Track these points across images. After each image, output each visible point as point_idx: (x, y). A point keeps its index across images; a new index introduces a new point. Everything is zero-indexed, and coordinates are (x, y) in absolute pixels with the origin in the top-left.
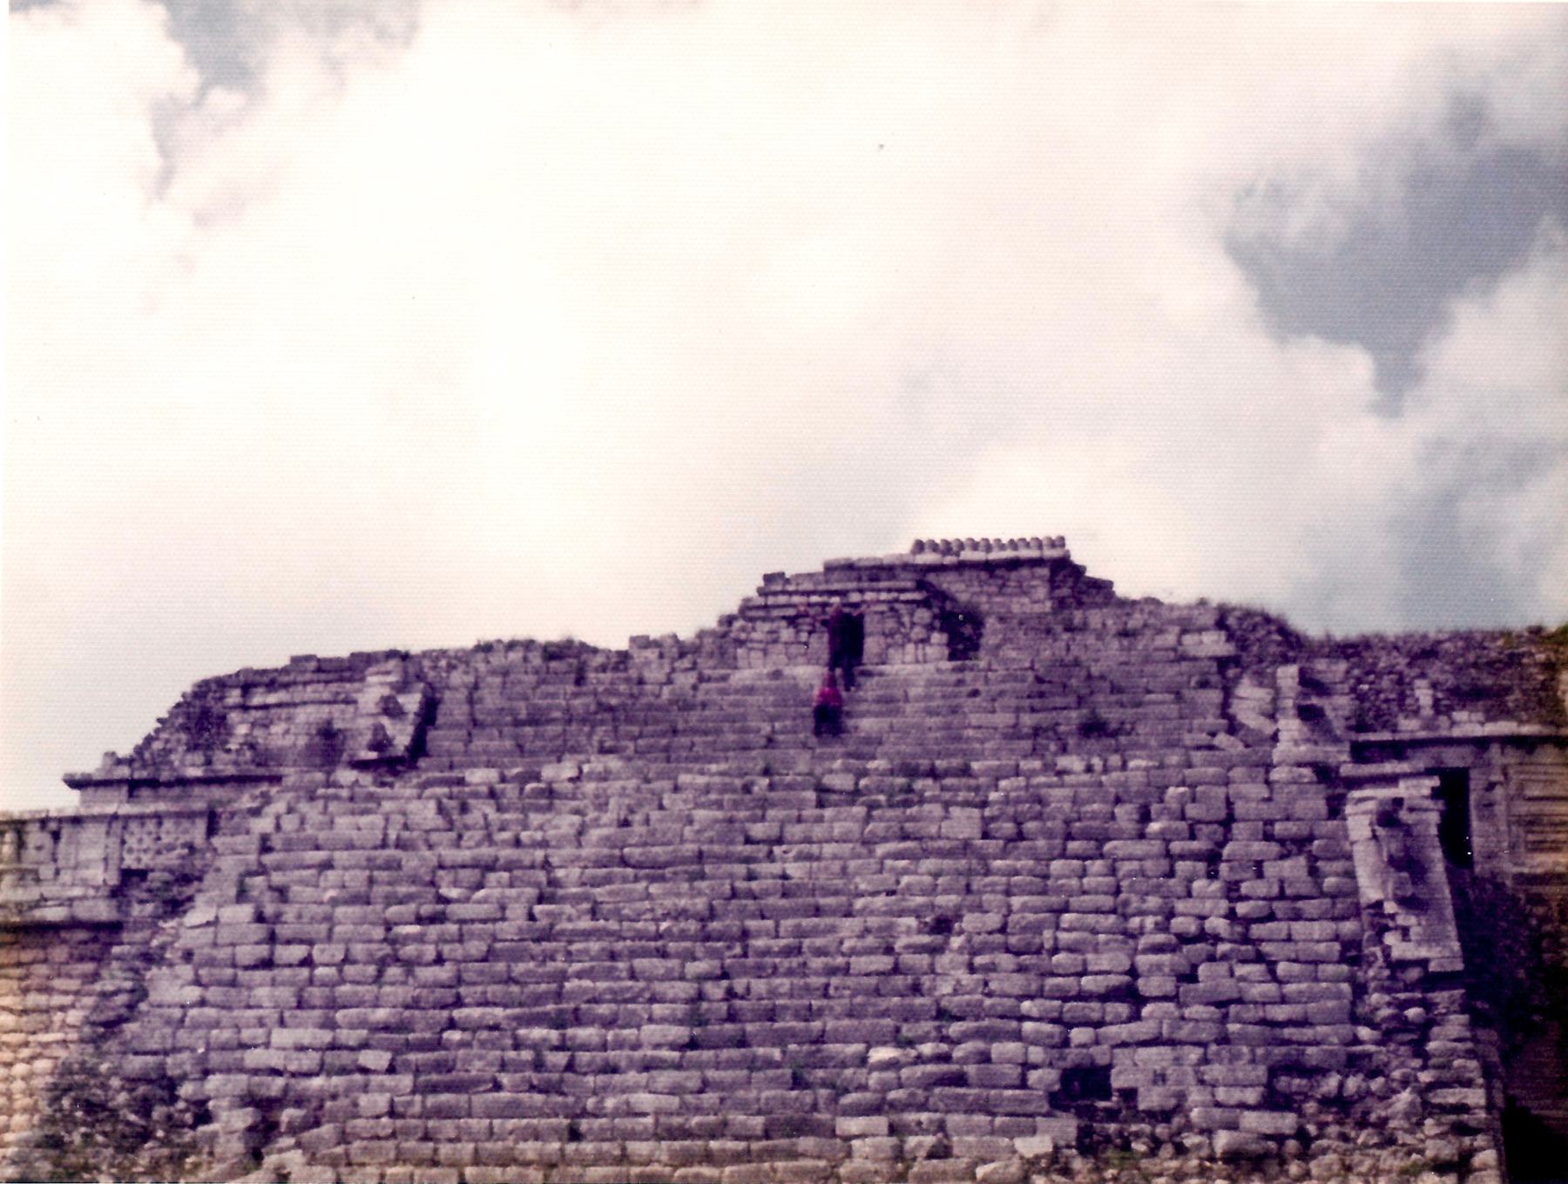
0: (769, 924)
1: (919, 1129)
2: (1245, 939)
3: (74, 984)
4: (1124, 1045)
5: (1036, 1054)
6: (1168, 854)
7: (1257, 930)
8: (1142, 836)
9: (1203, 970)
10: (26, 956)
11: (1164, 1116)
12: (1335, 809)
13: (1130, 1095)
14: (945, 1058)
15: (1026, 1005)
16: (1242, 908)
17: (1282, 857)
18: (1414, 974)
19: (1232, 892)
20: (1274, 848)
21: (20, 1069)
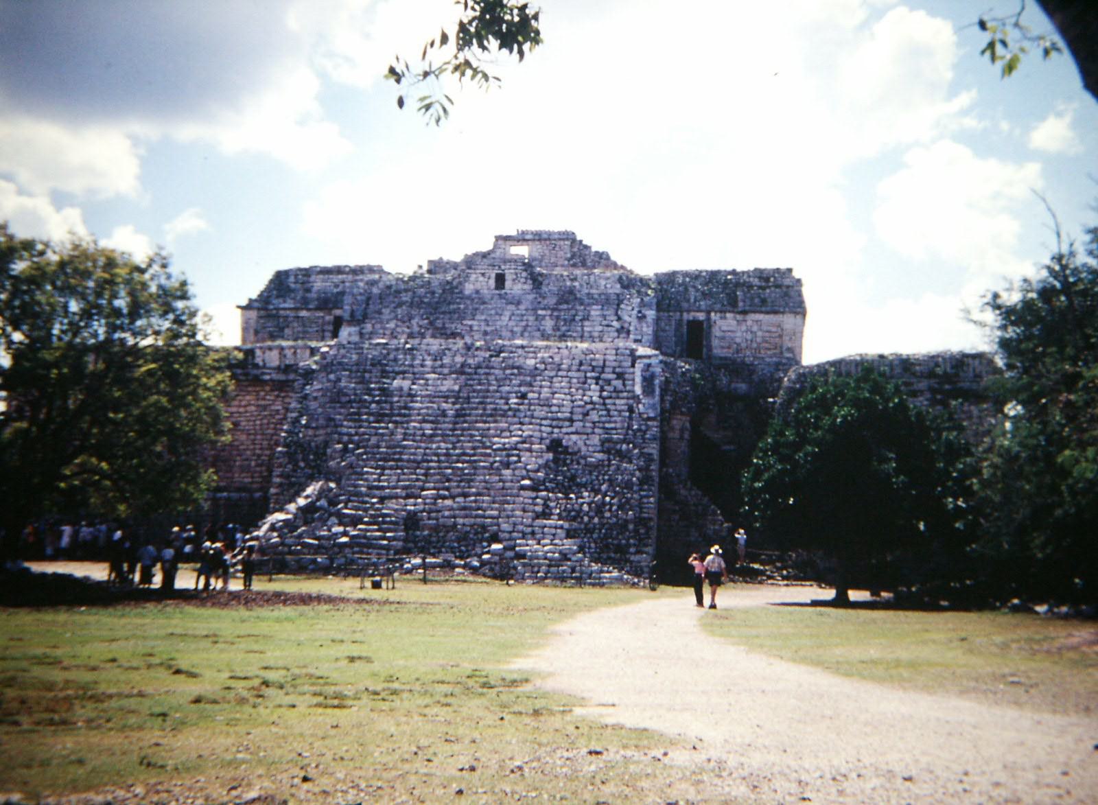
0: (475, 394)
1: (513, 455)
2: (604, 404)
3: (272, 398)
4: (567, 433)
5: (545, 435)
6: (586, 377)
7: (608, 401)
8: (579, 370)
9: (591, 412)
10: (258, 389)
11: (575, 453)
12: (633, 366)
13: (567, 447)
14: (521, 436)
15: (544, 422)
16: (605, 394)
17: (616, 379)
18: (645, 416)
19: (602, 390)
20: (615, 376)
21: (258, 422)
